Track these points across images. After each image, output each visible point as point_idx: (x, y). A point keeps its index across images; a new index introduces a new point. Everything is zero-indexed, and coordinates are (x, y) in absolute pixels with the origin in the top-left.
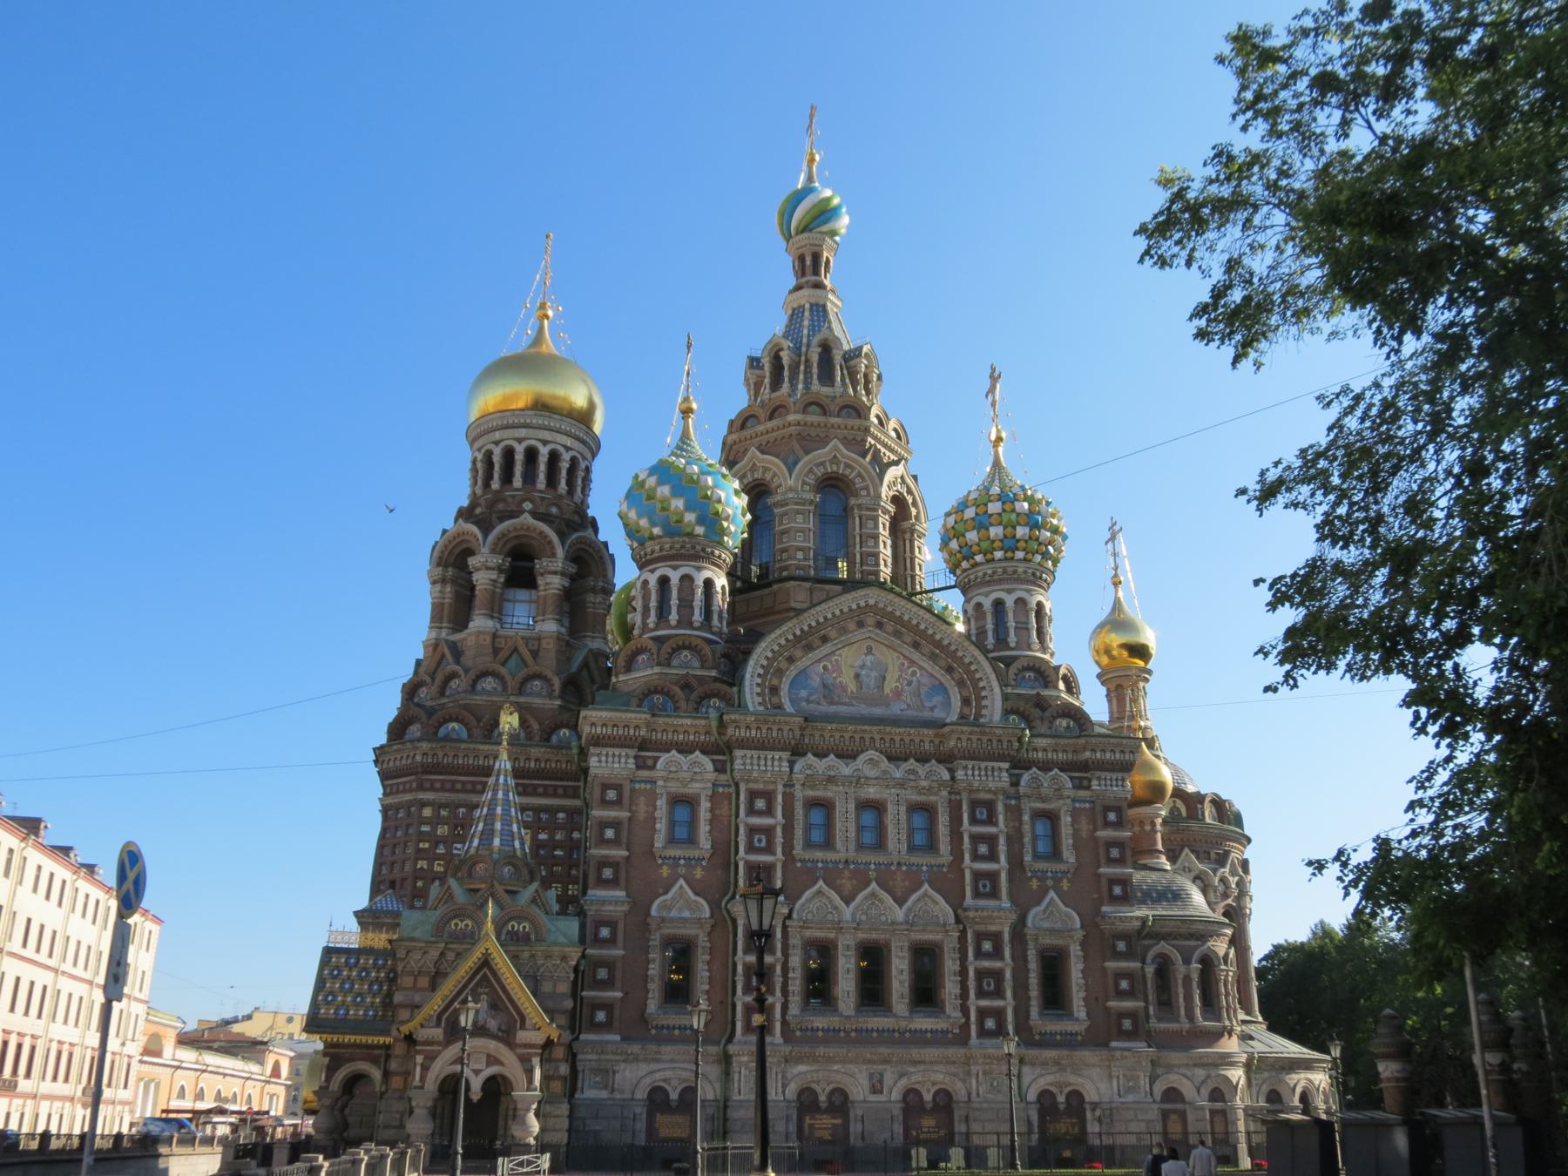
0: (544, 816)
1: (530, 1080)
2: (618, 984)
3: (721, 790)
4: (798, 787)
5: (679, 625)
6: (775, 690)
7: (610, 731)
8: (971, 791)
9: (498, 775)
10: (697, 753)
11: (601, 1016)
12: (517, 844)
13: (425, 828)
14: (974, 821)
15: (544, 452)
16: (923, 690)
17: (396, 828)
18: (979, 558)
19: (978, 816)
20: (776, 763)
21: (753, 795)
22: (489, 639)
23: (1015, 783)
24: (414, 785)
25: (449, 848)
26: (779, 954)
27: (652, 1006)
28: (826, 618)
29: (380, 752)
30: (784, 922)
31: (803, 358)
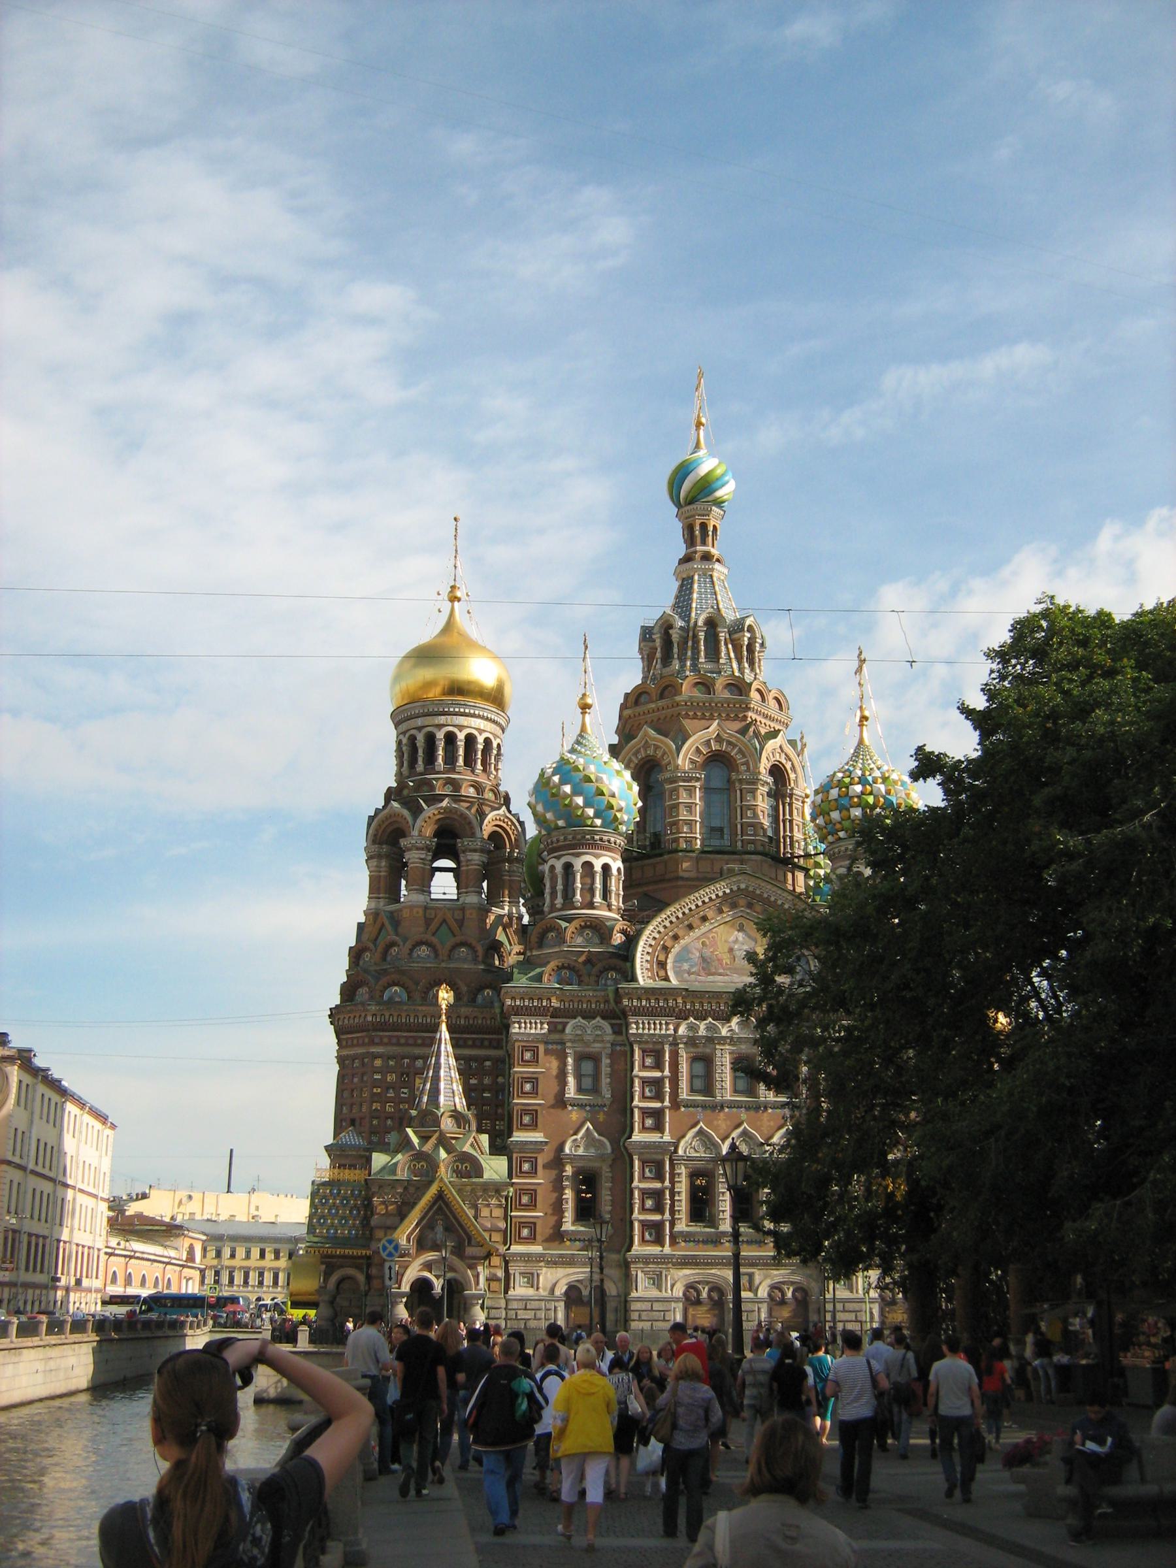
0: (474, 1065)
1: (477, 1283)
3: (618, 1048)
6: (662, 965)
10: (598, 1019)
11: (525, 1232)
12: (457, 1100)
15: (461, 736)
17: (353, 1076)
18: (842, 834)
22: (421, 911)
24: (366, 1040)
26: (667, 1183)
28: (704, 902)
29: (334, 1014)
31: (691, 634)
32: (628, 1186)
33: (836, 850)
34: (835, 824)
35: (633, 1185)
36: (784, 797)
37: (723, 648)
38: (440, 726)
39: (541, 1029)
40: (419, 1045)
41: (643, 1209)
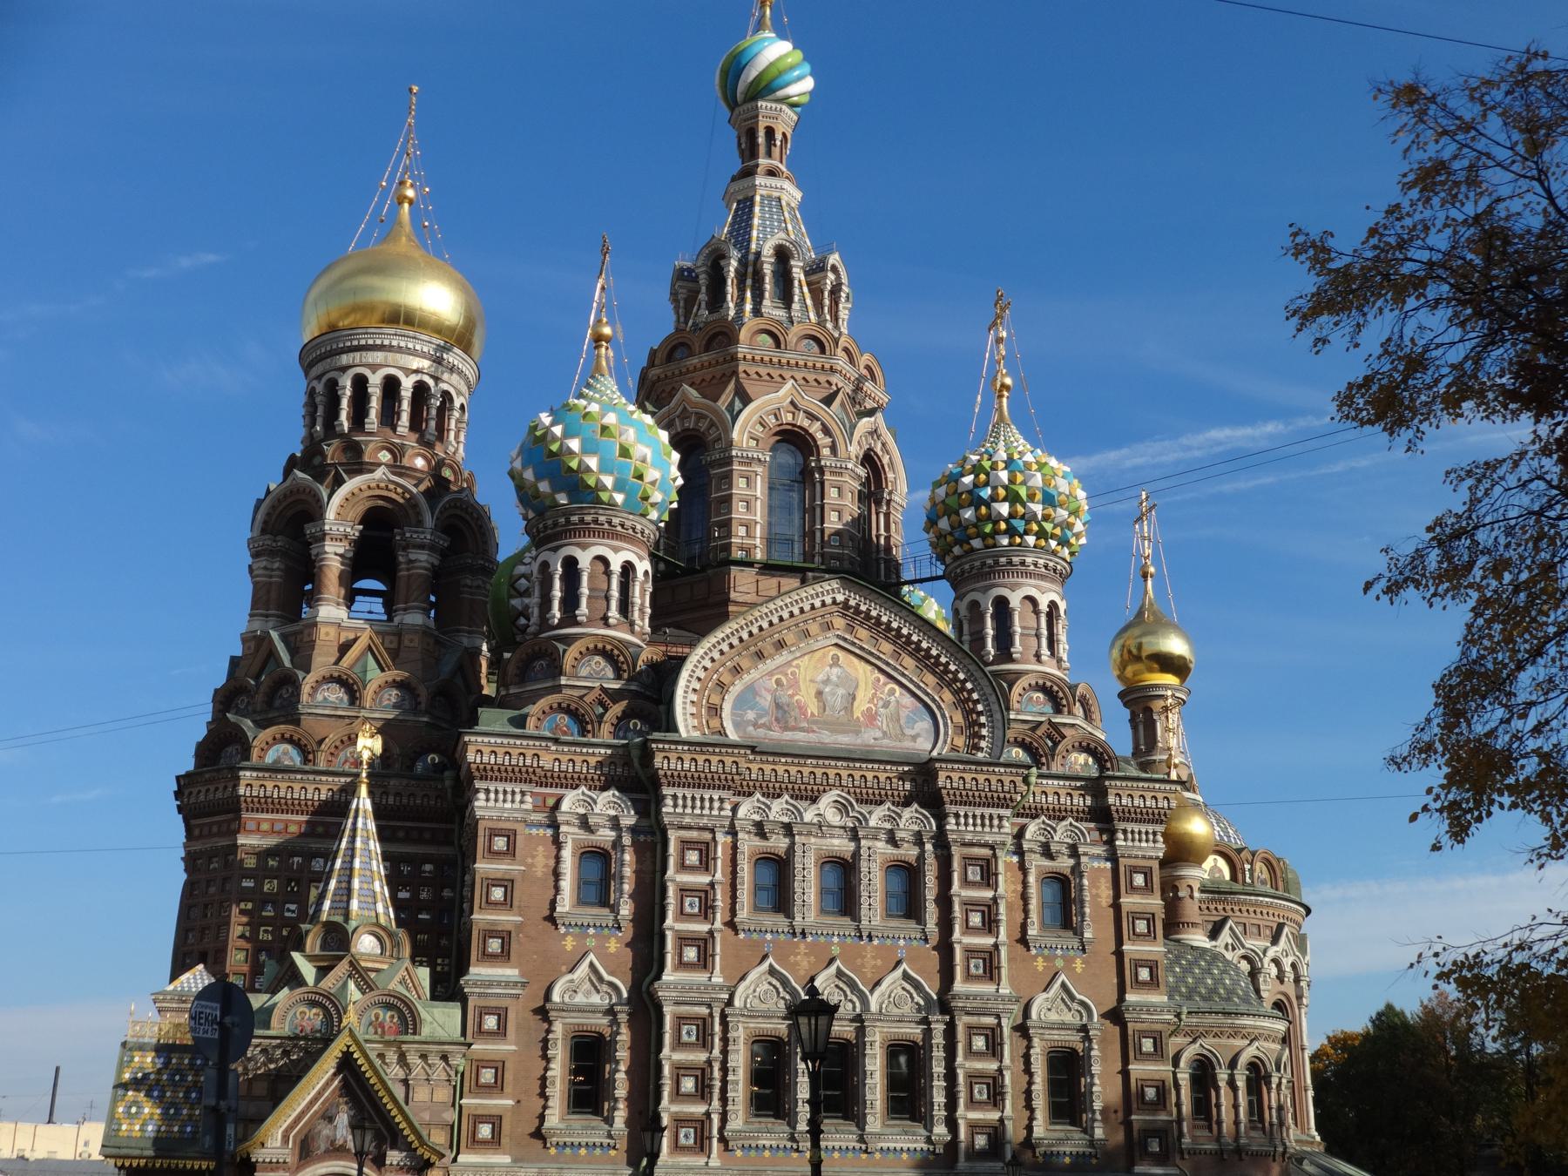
0: (406, 869)
2: (508, 1088)
3: (642, 838)
4: (740, 835)
5: (590, 622)
6: (715, 711)
7: (500, 761)
8: (964, 844)
9: (356, 817)
12: (380, 908)
13: (248, 883)
14: (966, 882)
15: (407, 384)
16: (904, 713)
18: (977, 543)
19: (971, 877)
20: (716, 805)
21: (686, 844)
23: (1019, 835)
25: (279, 909)
26: (716, 1052)
27: (553, 1119)
29: (185, 785)
30: (723, 1011)
31: (750, 269)
32: (652, 1056)
33: (967, 567)
34: (966, 528)
35: (662, 1056)
36: (878, 503)
37: (797, 291)
38: (374, 368)
39: (522, 802)
40: (320, 836)
41: (677, 1094)
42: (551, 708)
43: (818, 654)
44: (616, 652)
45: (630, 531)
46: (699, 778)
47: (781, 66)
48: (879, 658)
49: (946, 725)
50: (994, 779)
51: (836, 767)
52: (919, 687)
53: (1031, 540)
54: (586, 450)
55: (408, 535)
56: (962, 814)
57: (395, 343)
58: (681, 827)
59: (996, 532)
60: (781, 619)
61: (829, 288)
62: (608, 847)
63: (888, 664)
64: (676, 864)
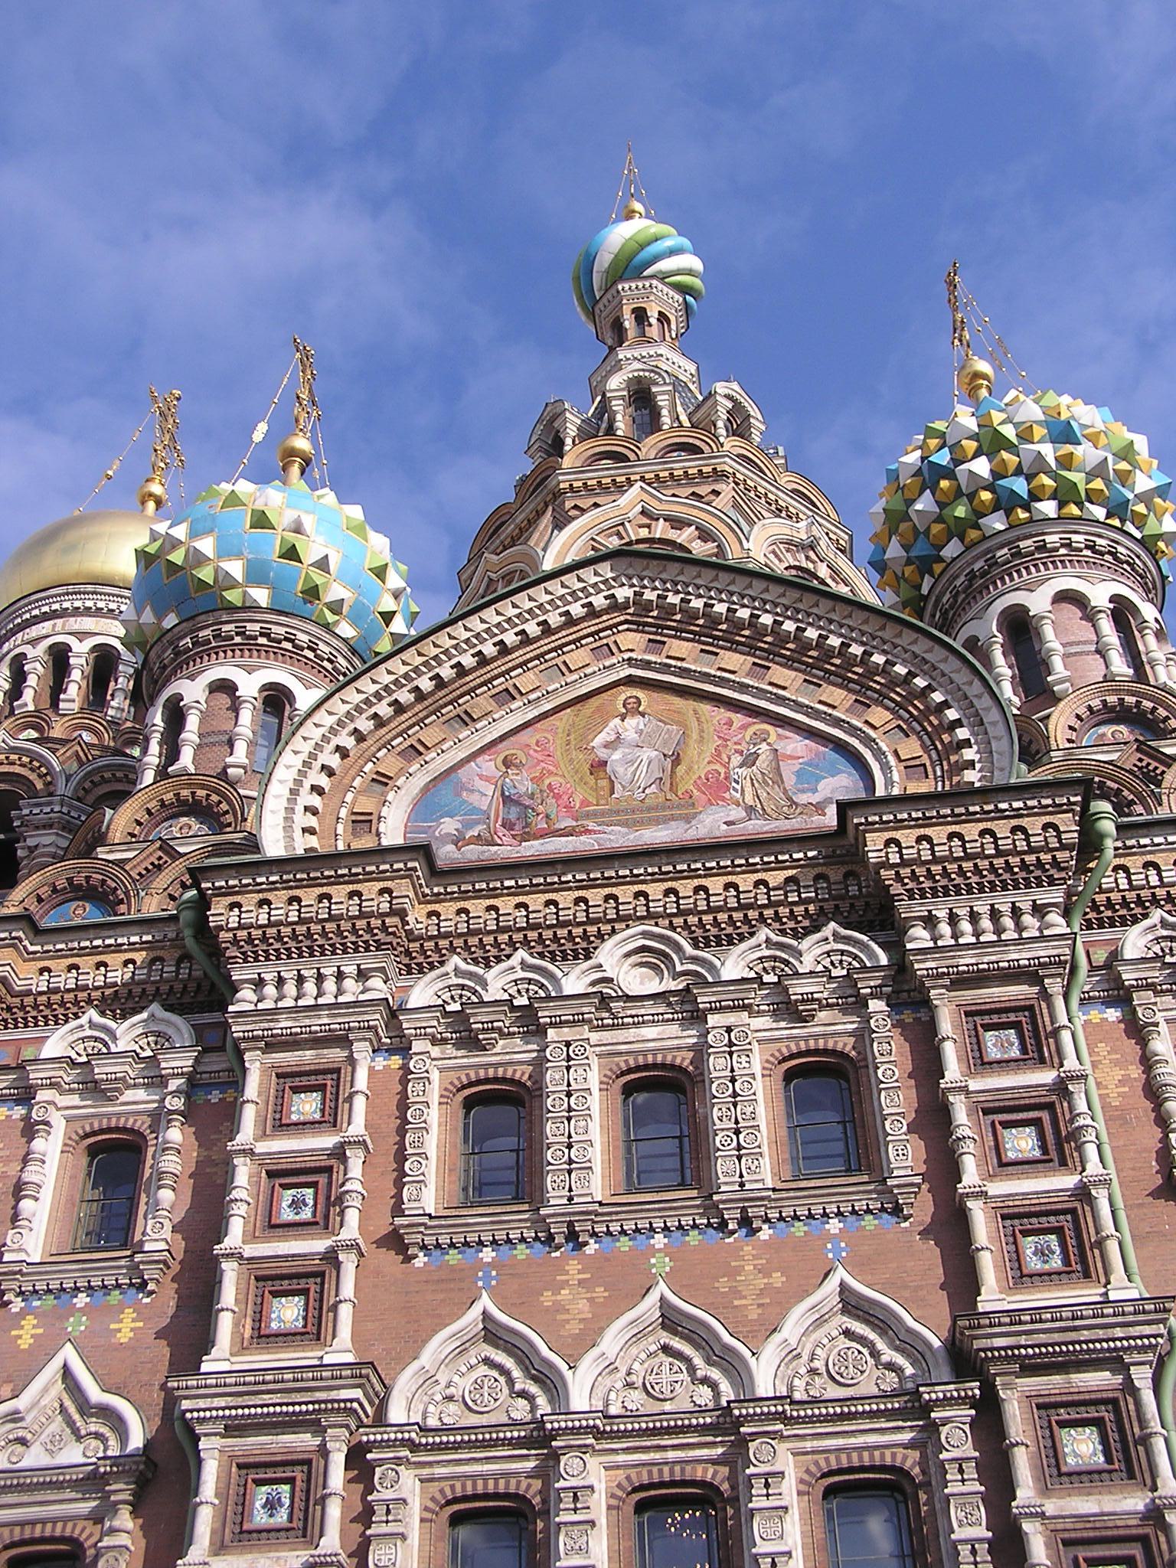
3: (215, 1097)
4: (417, 1046)
6: (364, 822)
8: (962, 981)
14: (980, 1063)
19: (993, 1053)
20: (349, 984)
38: (34, 642)
42: (55, 890)
43: (595, 702)
44: (215, 798)
45: (288, 646)
46: (309, 935)
47: (641, 238)
48: (722, 682)
49: (886, 768)
50: (1002, 828)
51: (635, 880)
52: (816, 715)
53: (1049, 508)
54: (194, 534)
55: (26, 812)
56: (942, 914)
57: (66, 605)
58: (273, 1045)
59: (979, 513)
60: (504, 649)
61: (723, 415)
62: (142, 1124)
63: (743, 688)
64: (261, 1121)
